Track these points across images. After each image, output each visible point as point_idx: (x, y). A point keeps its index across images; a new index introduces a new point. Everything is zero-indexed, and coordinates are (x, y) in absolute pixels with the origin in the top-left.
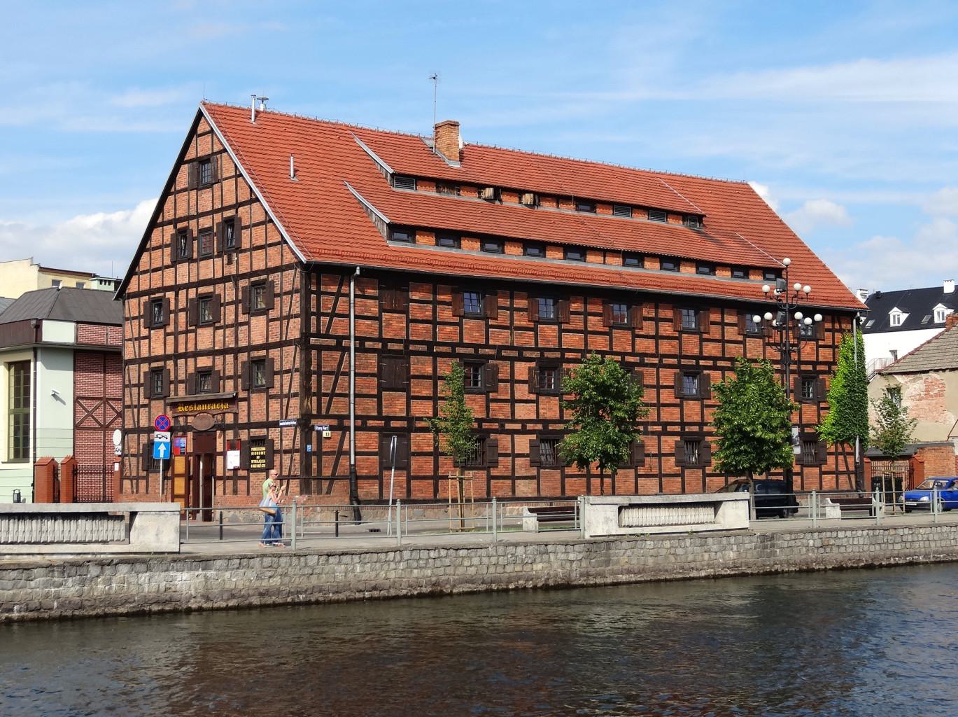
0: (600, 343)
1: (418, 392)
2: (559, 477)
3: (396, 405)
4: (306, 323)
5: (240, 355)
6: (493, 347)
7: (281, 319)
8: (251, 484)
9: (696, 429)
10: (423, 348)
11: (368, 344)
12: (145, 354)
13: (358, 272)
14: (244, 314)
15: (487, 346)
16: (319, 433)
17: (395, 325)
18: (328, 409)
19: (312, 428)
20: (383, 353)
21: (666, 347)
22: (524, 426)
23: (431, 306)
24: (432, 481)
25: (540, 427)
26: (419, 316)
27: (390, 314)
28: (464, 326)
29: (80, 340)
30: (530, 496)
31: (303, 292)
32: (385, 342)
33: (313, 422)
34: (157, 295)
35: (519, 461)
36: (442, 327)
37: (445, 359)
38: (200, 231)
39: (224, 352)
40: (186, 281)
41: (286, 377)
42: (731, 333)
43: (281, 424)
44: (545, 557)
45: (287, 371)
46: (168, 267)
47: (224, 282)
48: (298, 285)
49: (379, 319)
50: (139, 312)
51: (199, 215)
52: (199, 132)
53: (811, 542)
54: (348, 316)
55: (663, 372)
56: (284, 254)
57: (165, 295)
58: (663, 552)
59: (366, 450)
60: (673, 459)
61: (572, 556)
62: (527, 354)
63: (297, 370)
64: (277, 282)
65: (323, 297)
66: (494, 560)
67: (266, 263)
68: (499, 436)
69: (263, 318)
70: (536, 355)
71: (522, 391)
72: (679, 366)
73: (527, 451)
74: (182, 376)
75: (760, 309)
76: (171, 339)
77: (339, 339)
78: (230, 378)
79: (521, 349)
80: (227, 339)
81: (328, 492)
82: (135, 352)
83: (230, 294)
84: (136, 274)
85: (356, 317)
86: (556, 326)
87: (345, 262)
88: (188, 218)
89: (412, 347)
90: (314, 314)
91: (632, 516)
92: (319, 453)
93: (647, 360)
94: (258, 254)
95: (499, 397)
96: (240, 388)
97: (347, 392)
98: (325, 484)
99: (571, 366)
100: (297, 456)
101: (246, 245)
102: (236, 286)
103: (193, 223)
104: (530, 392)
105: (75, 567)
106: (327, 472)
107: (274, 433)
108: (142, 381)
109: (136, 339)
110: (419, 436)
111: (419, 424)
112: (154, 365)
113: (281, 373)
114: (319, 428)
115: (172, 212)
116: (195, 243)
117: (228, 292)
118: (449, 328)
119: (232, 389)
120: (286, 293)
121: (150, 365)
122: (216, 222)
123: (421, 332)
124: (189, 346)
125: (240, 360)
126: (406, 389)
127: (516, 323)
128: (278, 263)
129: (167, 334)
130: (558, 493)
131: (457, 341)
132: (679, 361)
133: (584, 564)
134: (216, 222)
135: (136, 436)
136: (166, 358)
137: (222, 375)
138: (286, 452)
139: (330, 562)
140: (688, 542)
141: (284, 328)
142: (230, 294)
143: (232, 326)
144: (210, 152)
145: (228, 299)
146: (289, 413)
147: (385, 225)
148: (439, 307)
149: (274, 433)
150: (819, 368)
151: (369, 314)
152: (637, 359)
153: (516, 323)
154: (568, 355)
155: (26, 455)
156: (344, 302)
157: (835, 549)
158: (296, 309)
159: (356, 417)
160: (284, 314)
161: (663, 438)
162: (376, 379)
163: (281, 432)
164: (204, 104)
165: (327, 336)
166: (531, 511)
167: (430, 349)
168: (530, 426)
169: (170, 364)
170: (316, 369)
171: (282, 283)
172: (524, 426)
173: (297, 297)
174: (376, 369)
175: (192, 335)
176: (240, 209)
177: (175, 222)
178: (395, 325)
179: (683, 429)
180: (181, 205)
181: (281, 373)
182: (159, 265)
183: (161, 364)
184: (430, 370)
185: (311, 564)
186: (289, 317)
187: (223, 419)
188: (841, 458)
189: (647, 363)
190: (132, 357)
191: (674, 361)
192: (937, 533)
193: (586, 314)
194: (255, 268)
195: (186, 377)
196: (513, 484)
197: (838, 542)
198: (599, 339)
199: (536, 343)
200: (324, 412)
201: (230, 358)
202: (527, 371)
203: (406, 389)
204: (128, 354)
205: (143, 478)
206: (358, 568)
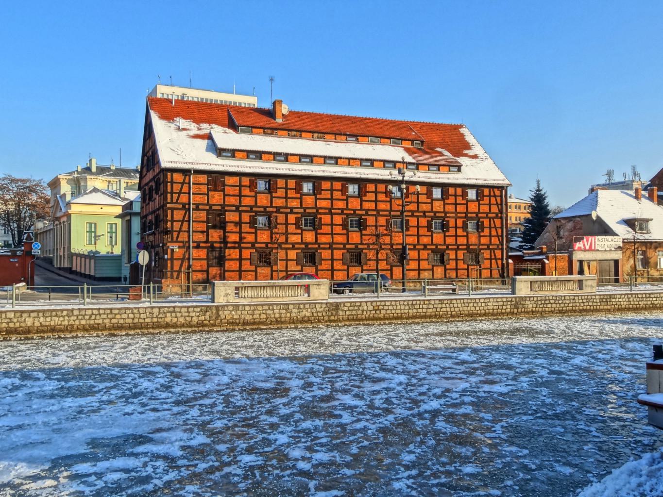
0: (341, 205)
6: (274, 207)
10: (234, 208)
11: (200, 207)
15: (271, 206)
16: (172, 250)
17: (216, 198)
18: (177, 238)
21: (381, 206)
25: (303, 246)
26: (231, 193)
44: (174, 315)
49: (208, 195)
54: (189, 193)
62: (295, 210)
70: (302, 211)
71: (292, 229)
72: (390, 215)
77: (184, 205)
79: (292, 209)
81: (177, 278)
85: (193, 194)
89: (226, 208)
93: (369, 213)
98: (175, 274)
99: (322, 216)
127: (289, 196)
140: (275, 307)
152: (364, 212)
154: (320, 211)
157: (383, 312)
159: (193, 242)
165: (177, 203)
168: (297, 246)
178: (216, 197)
179: (392, 247)
197: (386, 308)
199: (301, 205)
200: (175, 239)
206: (42, 319)
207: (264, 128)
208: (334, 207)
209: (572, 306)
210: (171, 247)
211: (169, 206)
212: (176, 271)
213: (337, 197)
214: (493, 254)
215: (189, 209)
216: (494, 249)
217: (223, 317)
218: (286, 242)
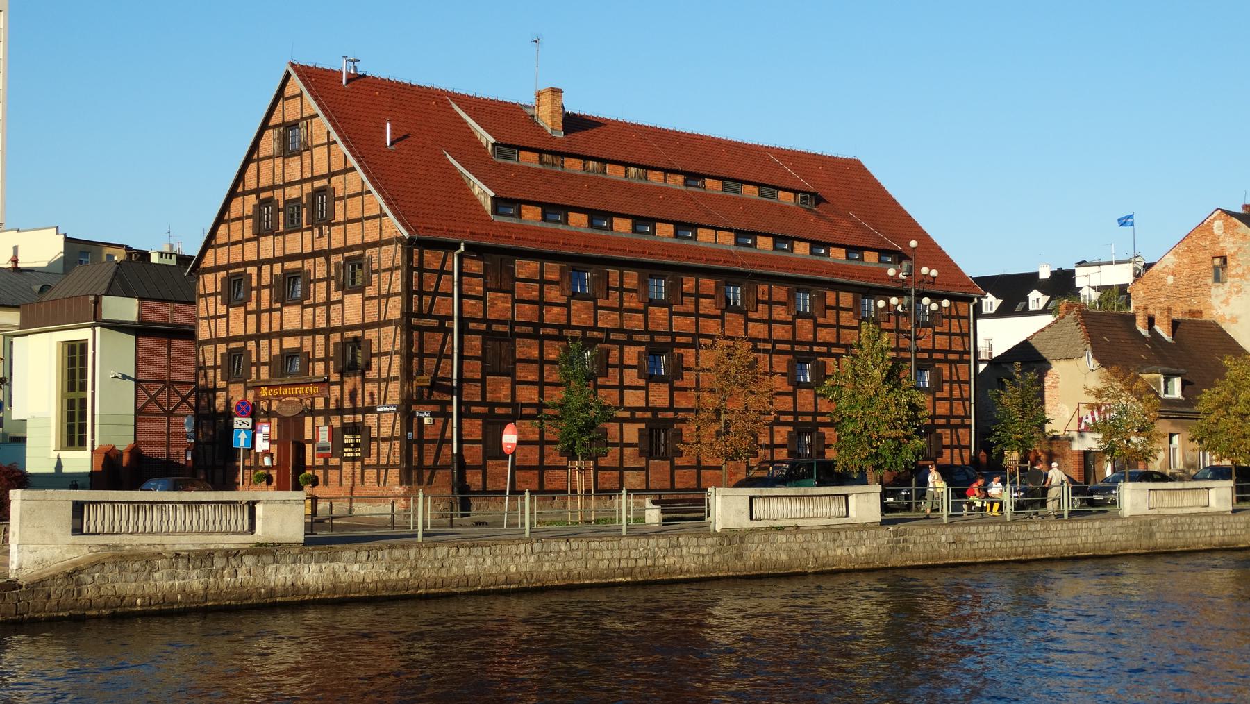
1: (524, 377)
2: (668, 467)
3: (501, 390)
4: (408, 302)
5: (332, 336)
6: (601, 330)
7: (379, 297)
8: (344, 474)
9: (809, 419)
12: (222, 333)
13: (462, 248)
14: (336, 290)
15: (595, 328)
16: (421, 419)
17: (500, 305)
19: (414, 413)
20: (488, 335)
21: (779, 332)
22: (633, 415)
23: (538, 285)
24: (536, 472)
25: (649, 415)
26: (526, 296)
27: (495, 294)
28: (572, 307)
29: (146, 318)
30: (638, 488)
31: (405, 269)
32: (490, 323)
33: (414, 407)
34: (237, 270)
35: (627, 451)
36: (548, 308)
37: (552, 342)
38: (286, 202)
39: (314, 332)
40: (270, 255)
41: (385, 360)
42: (846, 318)
43: (379, 410)
45: (386, 354)
46: (249, 240)
47: (314, 258)
48: (398, 261)
49: (483, 298)
50: (216, 289)
51: (285, 185)
52: (286, 95)
53: (943, 538)
55: (776, 358)
56: (384, 228)
57: (246, 270)
58: (796, 547)
59: (470, 438)
60: (785, 451)
61: (704, 550)
62: (637, 338)
63: (397, 352)
64: (376, 258)
65: (426, 275)
66: (625, 554)
67: (363, 237)
68: (607, 425)
69: (358, 297)
70: (645, 338)
72: (792, 352)
73: (636, 441)
74: (265, 357)
75: (886, 293)
76: (252, 319)
78: (320, 360)
79: (630, 332)
80: (317, 319)
82: (211, 332)
83: (321, 272)
84: (212, 247)
86: (667, 309)
87: (451, 239)
88: (273, 187)
90: (415, 292)
91: (761, 508)
92: (420, 441)
94: (354, 229)
95: (607, 383)
96: (332, 371)
97: (450, 376)
98: (426, 475)
99: (682, 350)
100: (397, 444)
101: (339, 217)
102: (328, 261)
103: (278, 194)
104: (640, 377)
105: (205, 556)
106: (428, 461)
107: (371, 420)
108: (219, 363)
109: (212, 318)
110: (524, 424)
111: (527, 411)
112: (233, 345)
113: (379, 355)
114: (421, 415)
115: (255, 181)
116: (281, 214)
117: (319, 268)
118: (556, 310)
119: (322, 373)
120: (385, 270)
121: (228, 345)
122: (305, 192)
123: (527, 312)
124: (273, 325)
125: (332, 341)
126: (511, 373)
127: (626, 305)
128: (376, 238)
129: (247, 313)
130: (667, 485)
131: (565, 323)
132: (793, 348)
133: (717, 558)
134: (305, 192)
136: (246, 338)
137: (311, 357)
138: (384, 440)
139: (460, 554)
140: (820, 537)
141: (383, 307)
142: (321, 272)
143: (323, 304)
144: (299, 117)
145: (319, 276)
146: (388, 398)
147: (489, 199)
148: (546, 286)
149: (371, 420)
150: (935, 356)
151: (474, 294)
153: (626, 305)
154: (679, 339)
155: (82, 444)
156: (447, 280)
157: (968, 547)
158: (397, 287)
160: (383, 292)
161: (775, 428)
162: (480, 362)
163: (379, 419)
164: (292, 65)
165: (429, 315)
166: (654, 502)
167: (537, 331)
168: (639, 414)
169: (251, 345)
170: (417, 352)
171: (380, 258)
172: (633, 415)
173: (397, 275)
174: (480, 352)
175: (276, 314)
176: (333, 179)
177: (257, 192)
178: (500, 305)
180: (267, 173)
181: (379, 355)
182: (240, 238)
183: (241, 344)
184: (535, 354)
185: (440, 556)
186: (388, 296)
187: (313, 403)
188: (956, 451)
189: (760, 349)
190: (208, 336)
191: (787, 347)
192: (1069, 529)
193: (698, 296)
194: (350, 243)
195: (270, 358)
196: (621, 475)
198: (711, 322)
199: (646, 326)
200: (425, 398)
201: (320, 339)
202: (637, 355)
203: (511, 373)
204: (203, 332)
207: (540, 152)
208: (703, 331)
209: (1211, 536)
210: (418, 414)
211: (414, 321)
212: (427, 468)
213: (707, 312)
214: (955, 437)
215: (452, 330)
216: (957, 427)
217: (746, 554)
218: (621, 407)
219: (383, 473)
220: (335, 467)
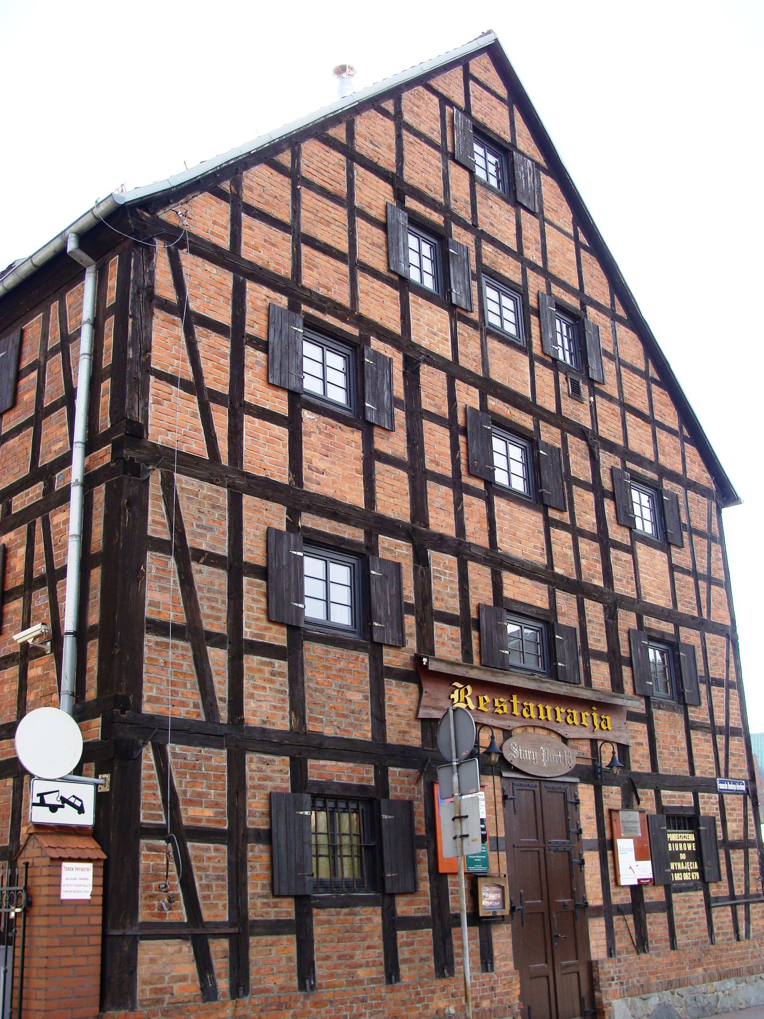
8: (677, 919)
34: (330, 319)
43: (721, 786)
80: (583, 562)
135: (219, 758)
149: (708, 805)
205: (275, 928)
219: (741, 912)
220: (656, 907)
